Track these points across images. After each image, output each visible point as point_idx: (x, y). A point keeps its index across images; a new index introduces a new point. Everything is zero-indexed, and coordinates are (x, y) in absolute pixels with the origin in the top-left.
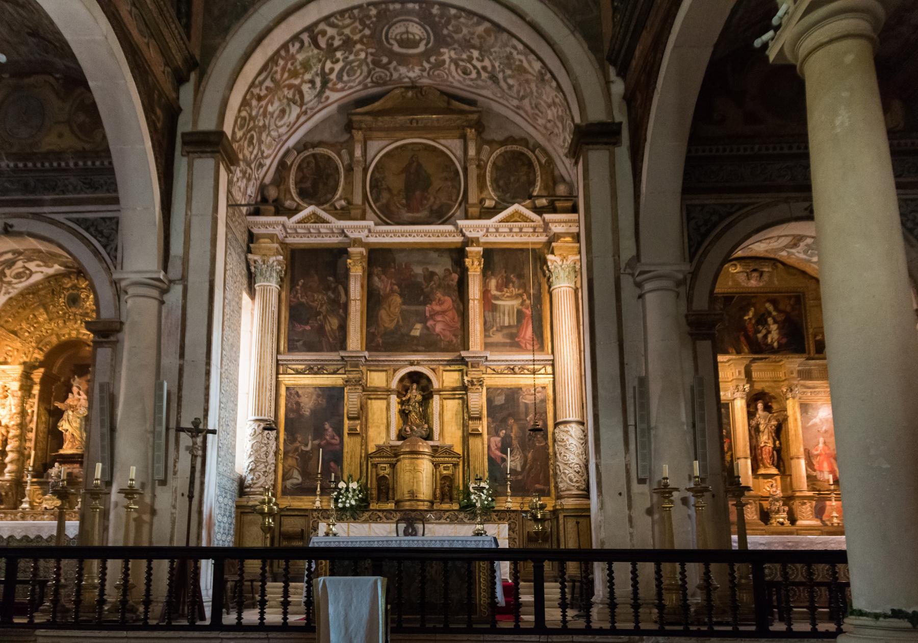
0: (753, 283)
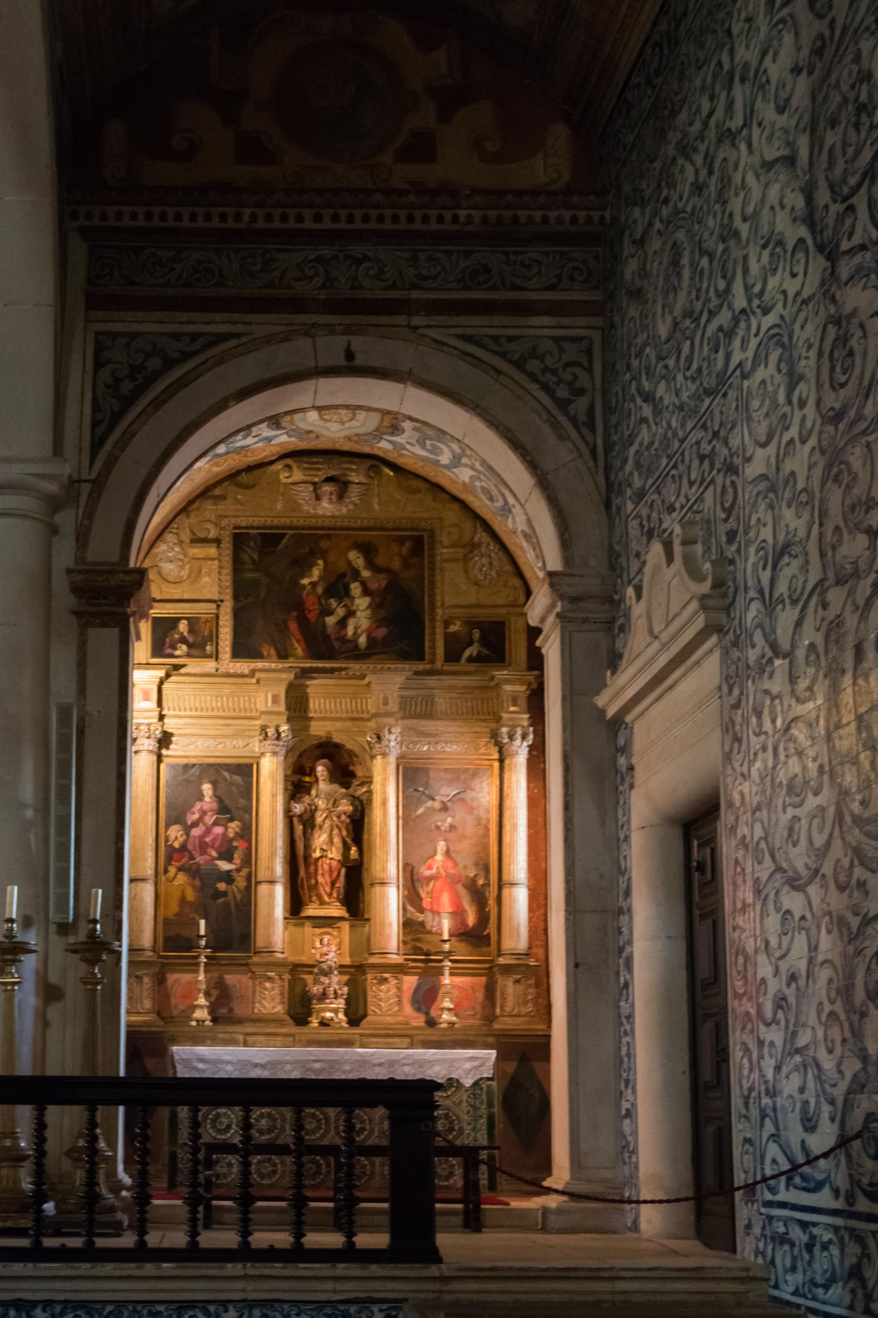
0: (327, 507)
